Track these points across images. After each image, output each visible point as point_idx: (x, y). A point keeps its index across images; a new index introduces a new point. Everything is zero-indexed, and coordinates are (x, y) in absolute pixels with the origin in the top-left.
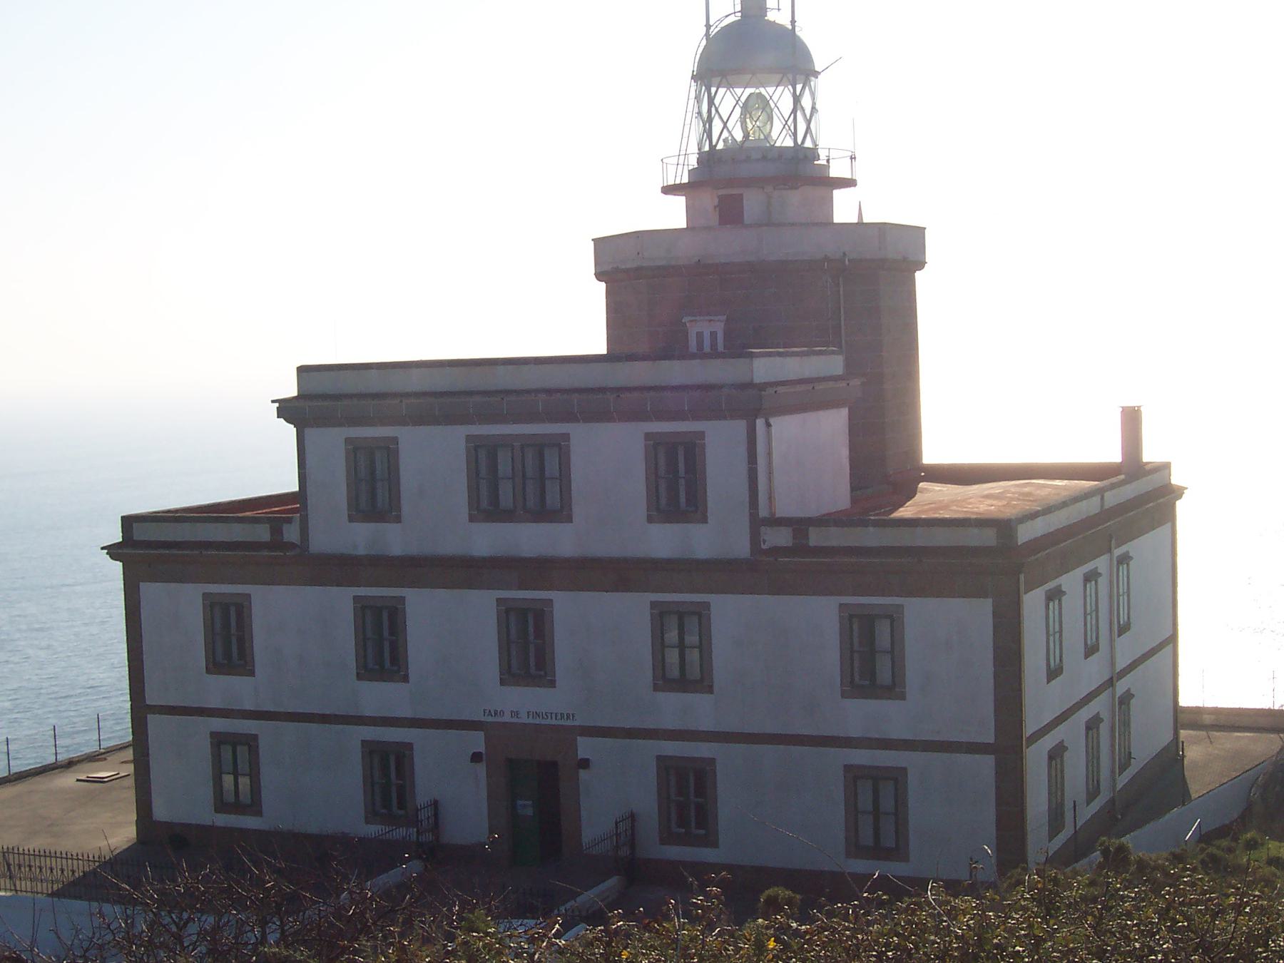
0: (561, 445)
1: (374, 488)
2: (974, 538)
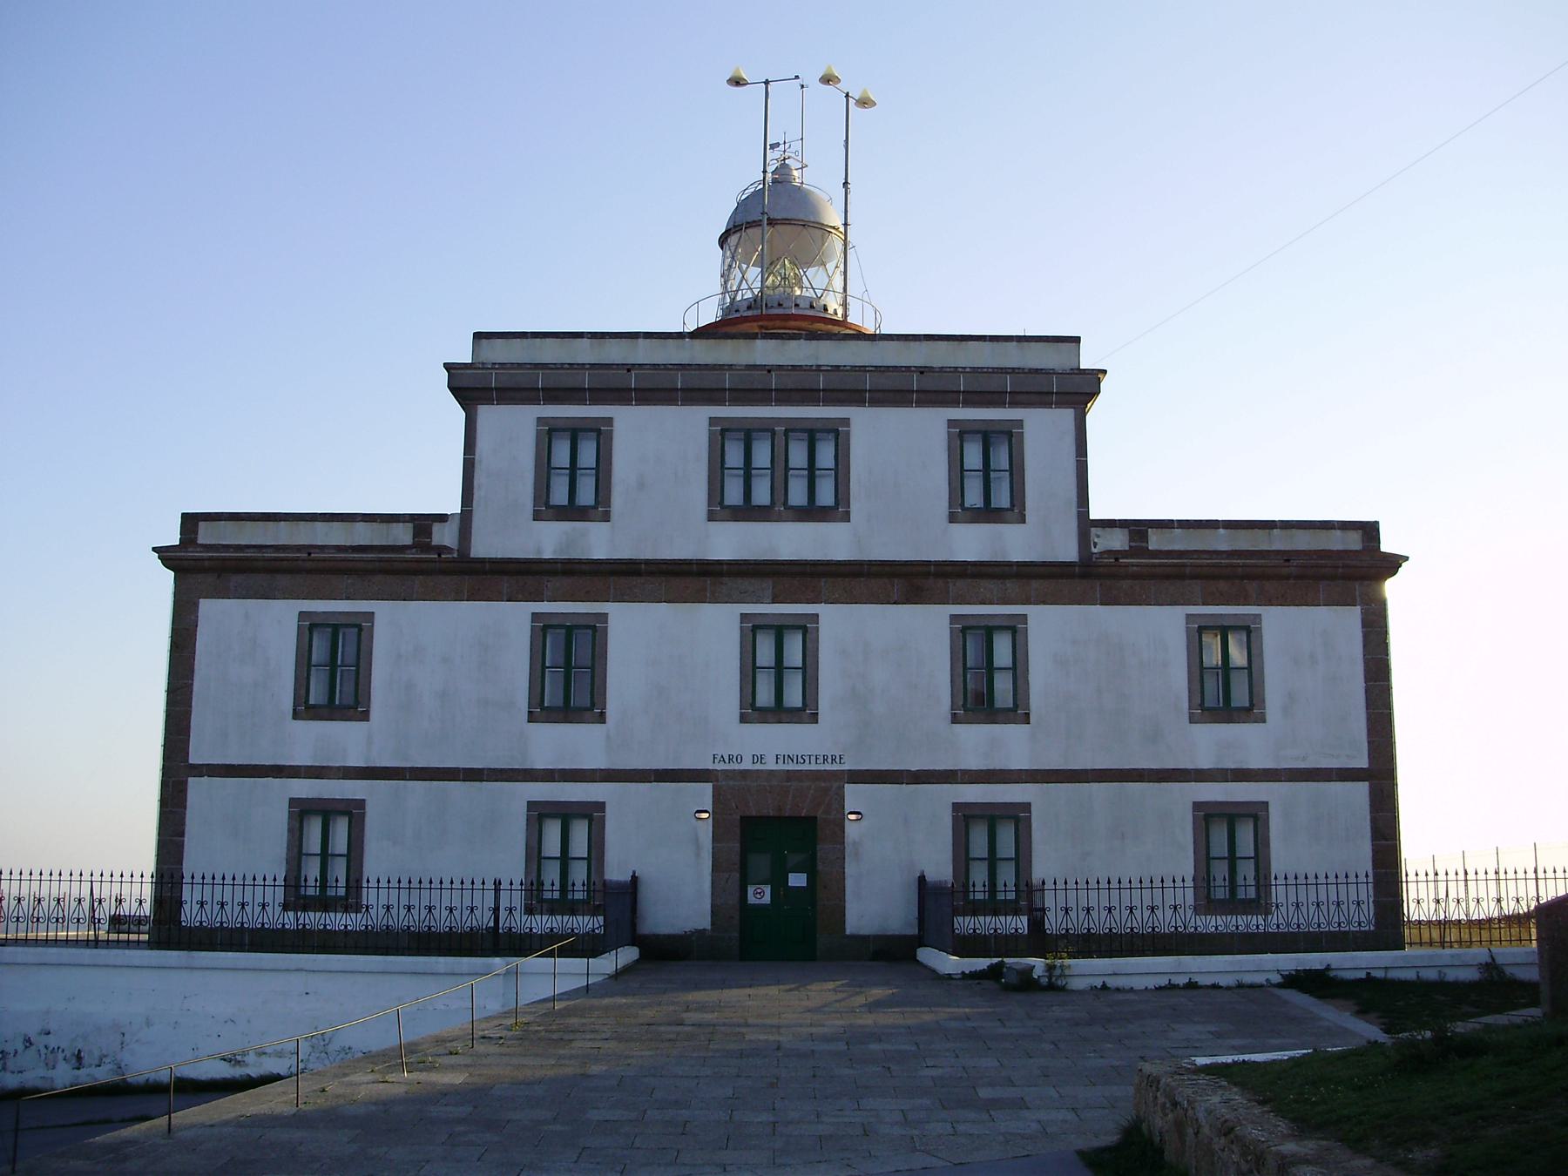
1: (574, 478)
2: (1336, 542)
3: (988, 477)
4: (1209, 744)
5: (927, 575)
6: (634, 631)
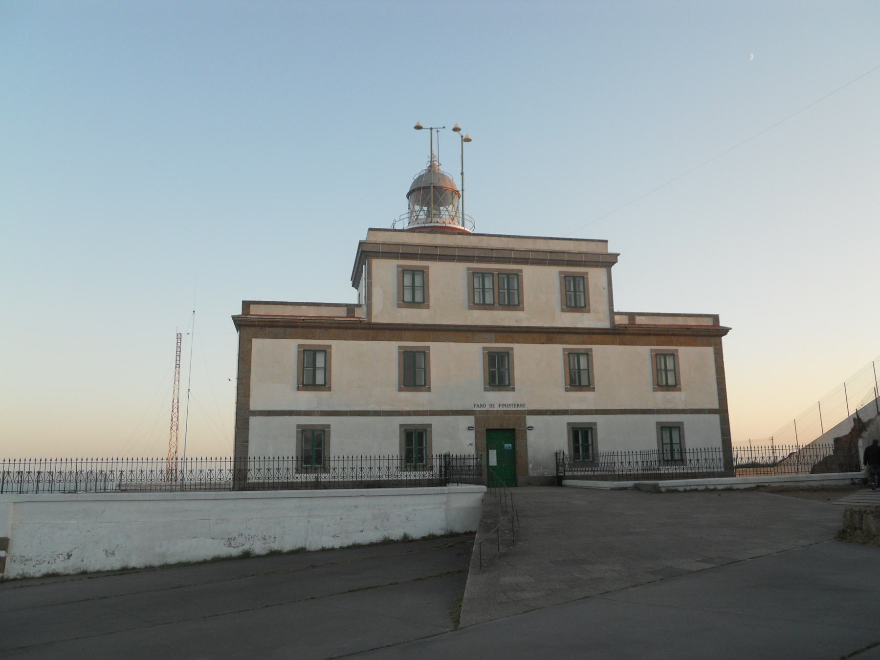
0: (518, 275)
1: (414, 291)
3: (575, 296)
4: (661, 399)
5: (554, 333)
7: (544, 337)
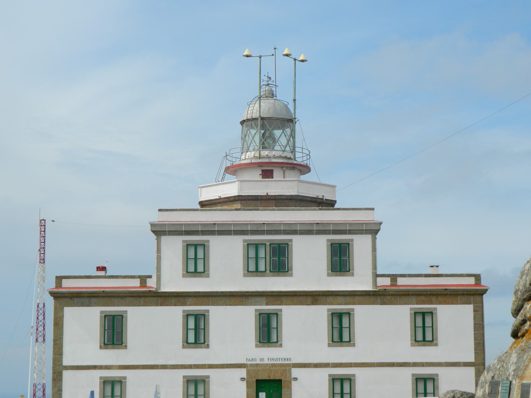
1: (196, 262)
3: (340, 260)
5: (319, 295)
6: (218, 315)
7: (310, 299)
